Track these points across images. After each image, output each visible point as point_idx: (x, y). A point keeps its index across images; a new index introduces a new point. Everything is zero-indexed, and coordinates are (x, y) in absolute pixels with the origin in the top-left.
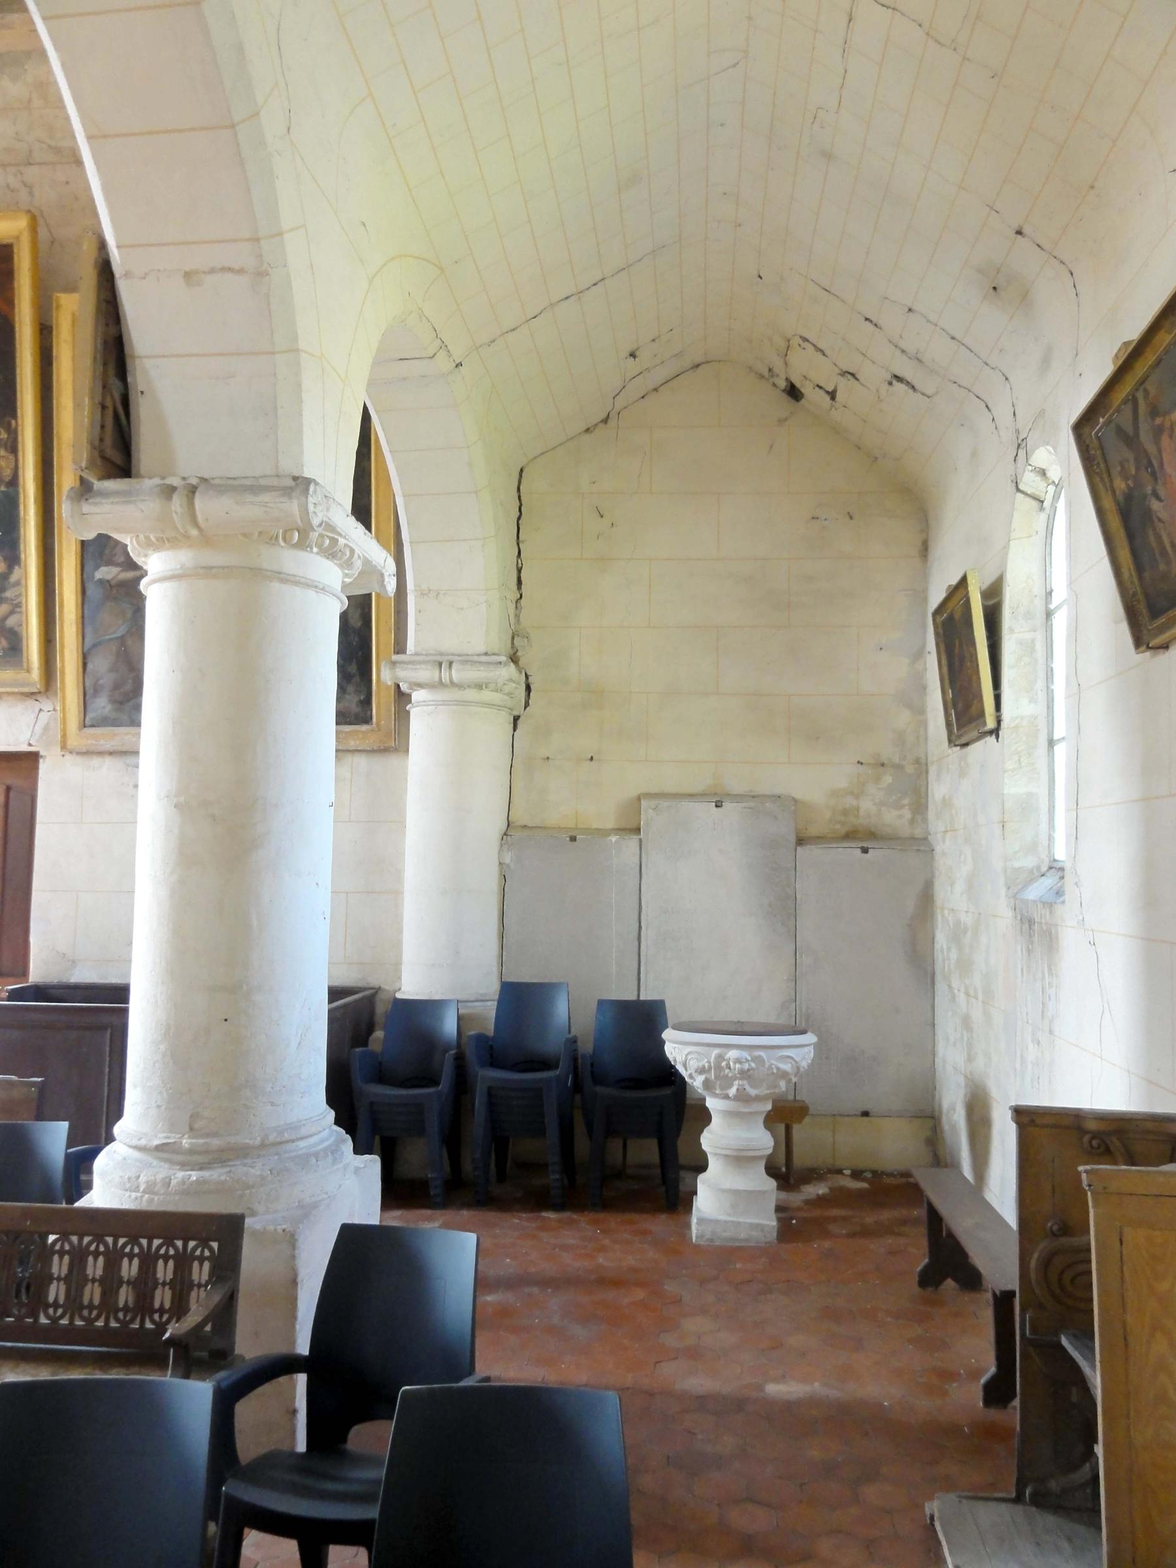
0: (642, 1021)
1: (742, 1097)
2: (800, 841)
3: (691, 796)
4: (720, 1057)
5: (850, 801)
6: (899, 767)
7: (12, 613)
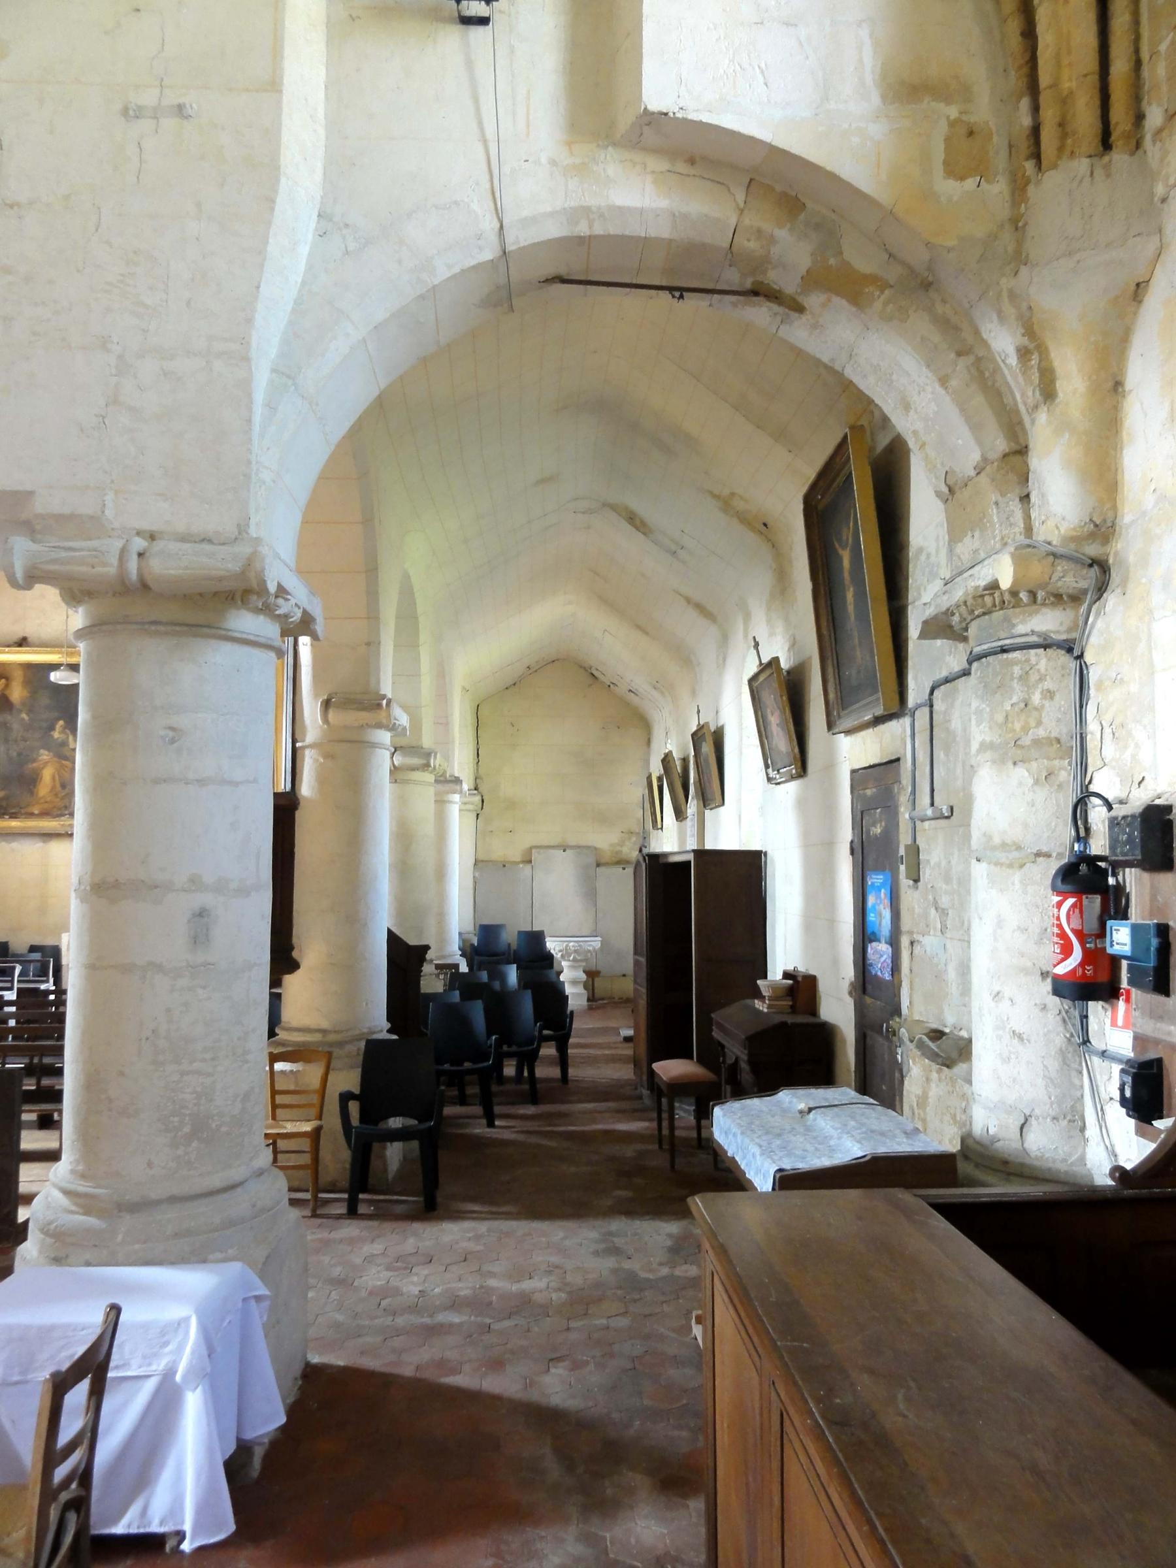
0: (535, 939)
1: (575, 960)
2: (598, 865)
5: (618, 848)
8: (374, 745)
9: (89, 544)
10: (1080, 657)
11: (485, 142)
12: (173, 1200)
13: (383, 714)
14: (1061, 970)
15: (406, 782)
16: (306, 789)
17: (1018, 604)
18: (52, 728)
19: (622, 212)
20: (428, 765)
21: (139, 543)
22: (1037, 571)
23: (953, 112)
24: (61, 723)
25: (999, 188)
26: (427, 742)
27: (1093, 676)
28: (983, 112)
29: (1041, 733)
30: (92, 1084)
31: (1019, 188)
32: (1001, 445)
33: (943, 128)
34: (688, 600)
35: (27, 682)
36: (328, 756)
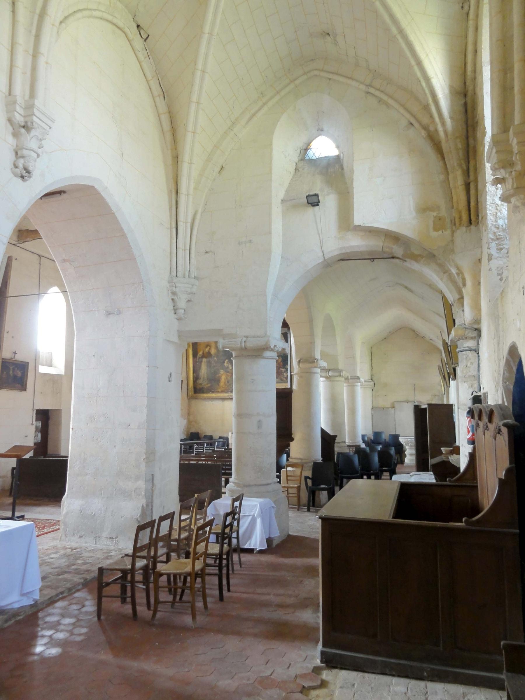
0: (396, 437)
1: (411, 446)
3: (403, 401)
6: (438, 396)
8: (314, 373)
9: (233, 340)
10: (478, 353)
11: (319, 234)
12: (255, 485)
13: (316, 364)
14: (468, 437)
15: (333, 381)
16: (294, 387)
17: (463, 339)
18: (224, 362)
19: (353, 247)
20: (340, 375)
21: (244, 339)
22: (460, 332)
23: (435, 214)
24: (227, 360)
25: (448, 232)
26: (340, 367)
27: (481, 358)
28: (443, 213)
29: (470, 374)
30: (238, 459)
31: (453, 232)
32: (457, 296)
33: (432, 218)
34: (434, 312)
36: (301, 377)
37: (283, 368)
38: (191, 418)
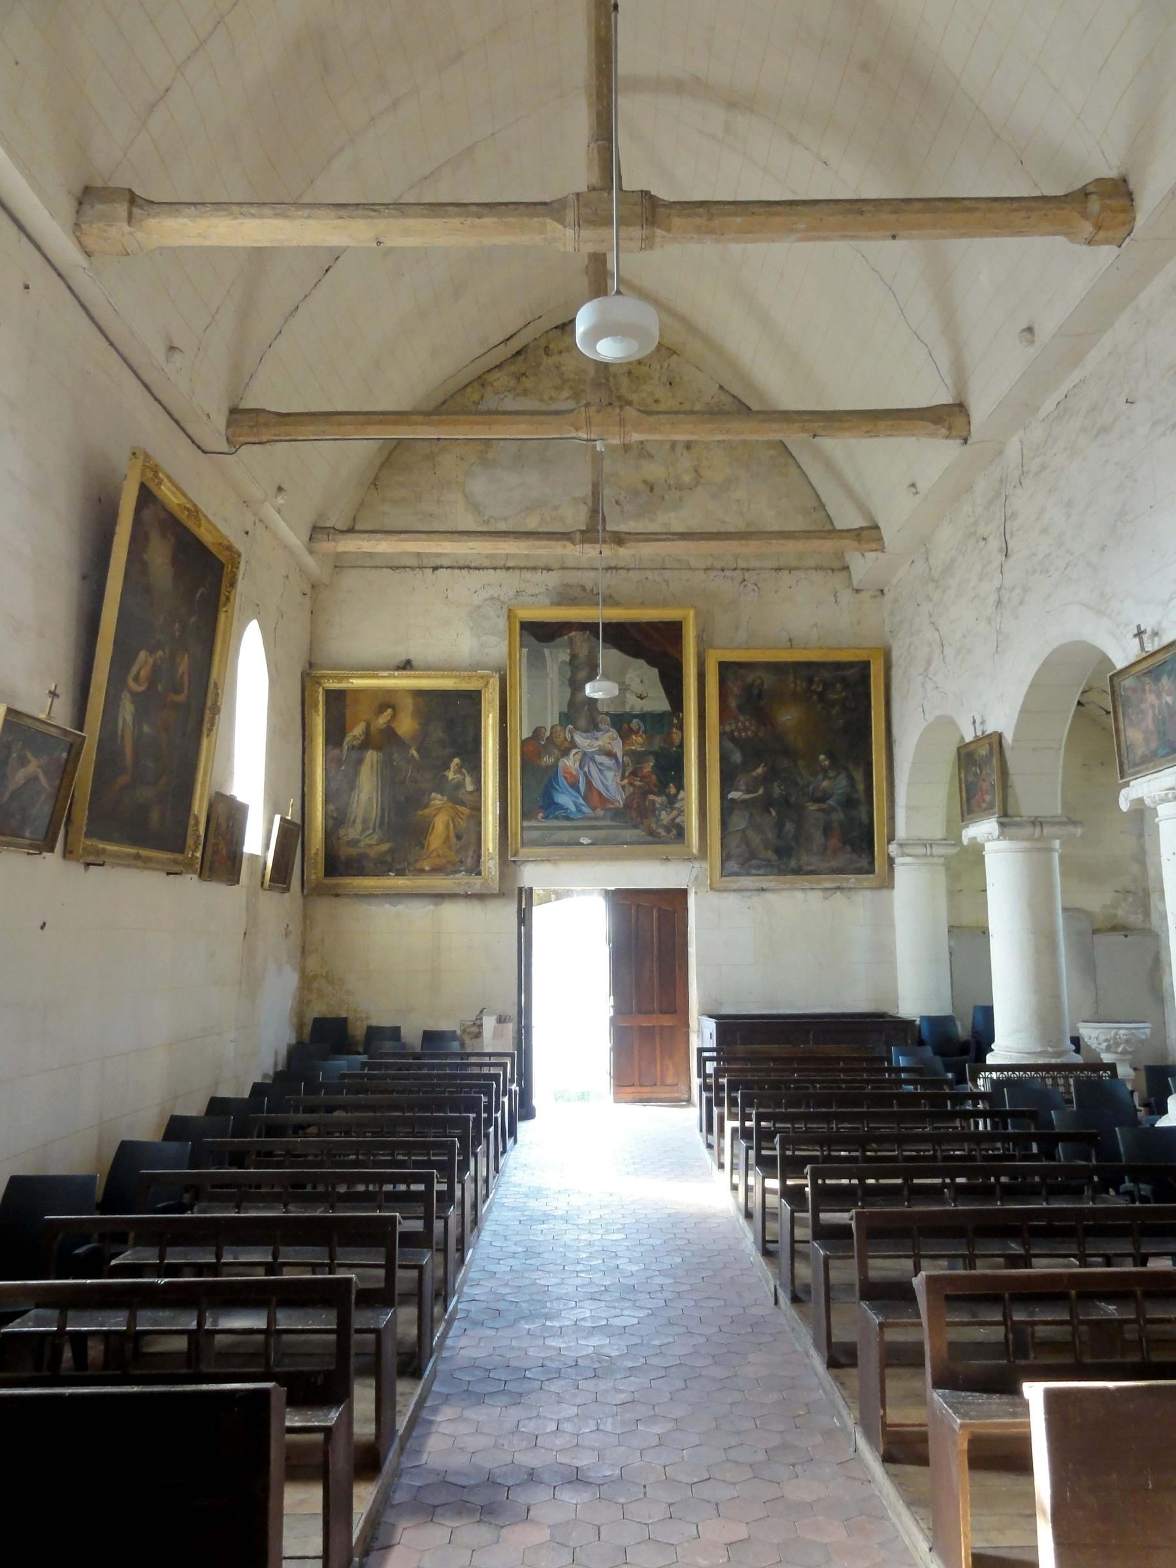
1: (1124, 1052)
2: (1095, 932)
4: (1116, 1034)
6: (1135, 893)
7: (679, 815)
24: (456, 760)
35: (417, 713)
37: (658, 794)
38: (313, 964)
